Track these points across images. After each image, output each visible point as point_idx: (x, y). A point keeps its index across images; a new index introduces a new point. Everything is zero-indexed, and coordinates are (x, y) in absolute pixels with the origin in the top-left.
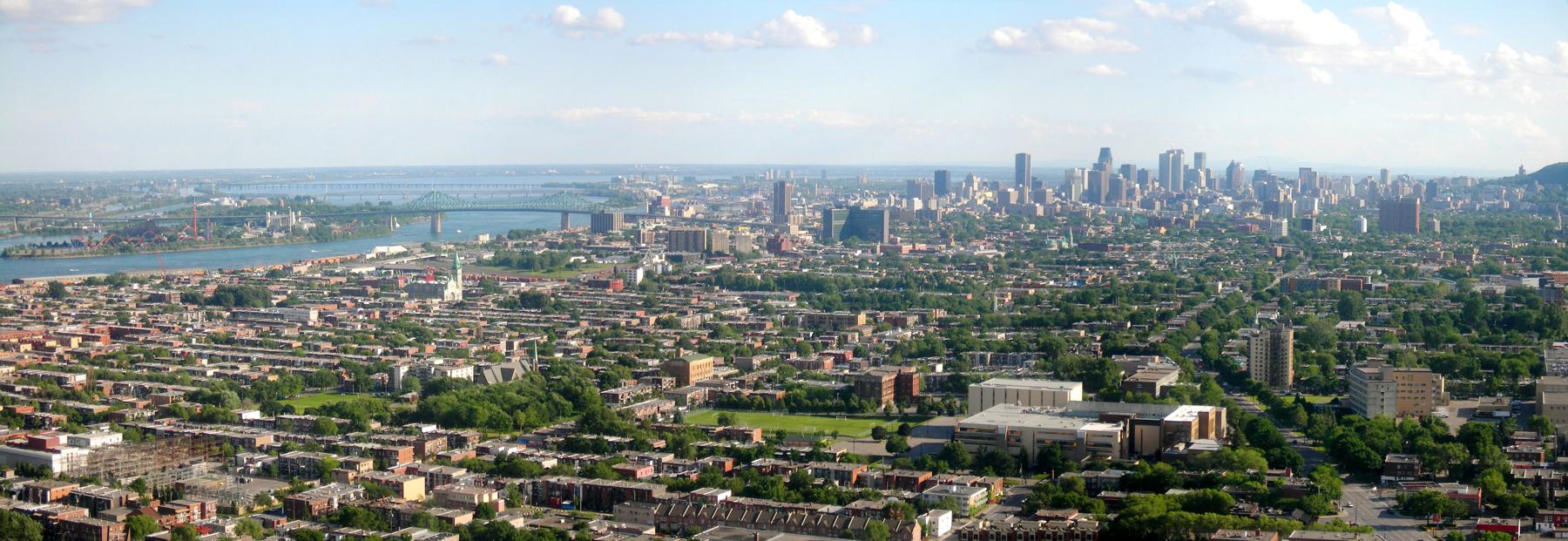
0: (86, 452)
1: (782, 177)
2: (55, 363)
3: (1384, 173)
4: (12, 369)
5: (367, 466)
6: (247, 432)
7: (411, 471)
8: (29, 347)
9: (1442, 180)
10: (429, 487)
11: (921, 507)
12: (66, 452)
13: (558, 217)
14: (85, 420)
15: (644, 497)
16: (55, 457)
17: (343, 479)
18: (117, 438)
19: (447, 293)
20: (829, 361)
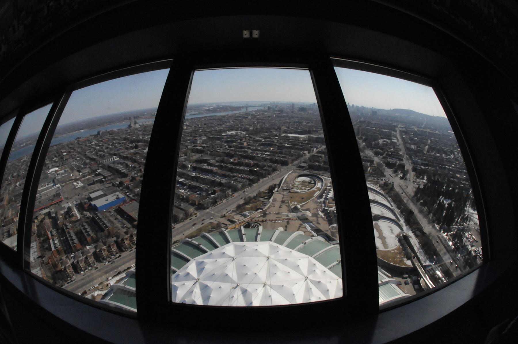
0: (202, 140)
1: (293, 103)
2: (197, 129)
3: (373, 107)
4: (191, 130)
5: (239, 141)
6: (223, 137)
7: (245, 141)
8: (193, 127)
9: (380, 109)
10: (247, 144)
11: (311, 147)
12: (199, 140)
13: (263, 108)
14: (200, 136)
15: (276, 145)
16: (198, 141)
17: (235, 142)
18: (206, 138)
19: (249, 118)
20: (300, 127)
